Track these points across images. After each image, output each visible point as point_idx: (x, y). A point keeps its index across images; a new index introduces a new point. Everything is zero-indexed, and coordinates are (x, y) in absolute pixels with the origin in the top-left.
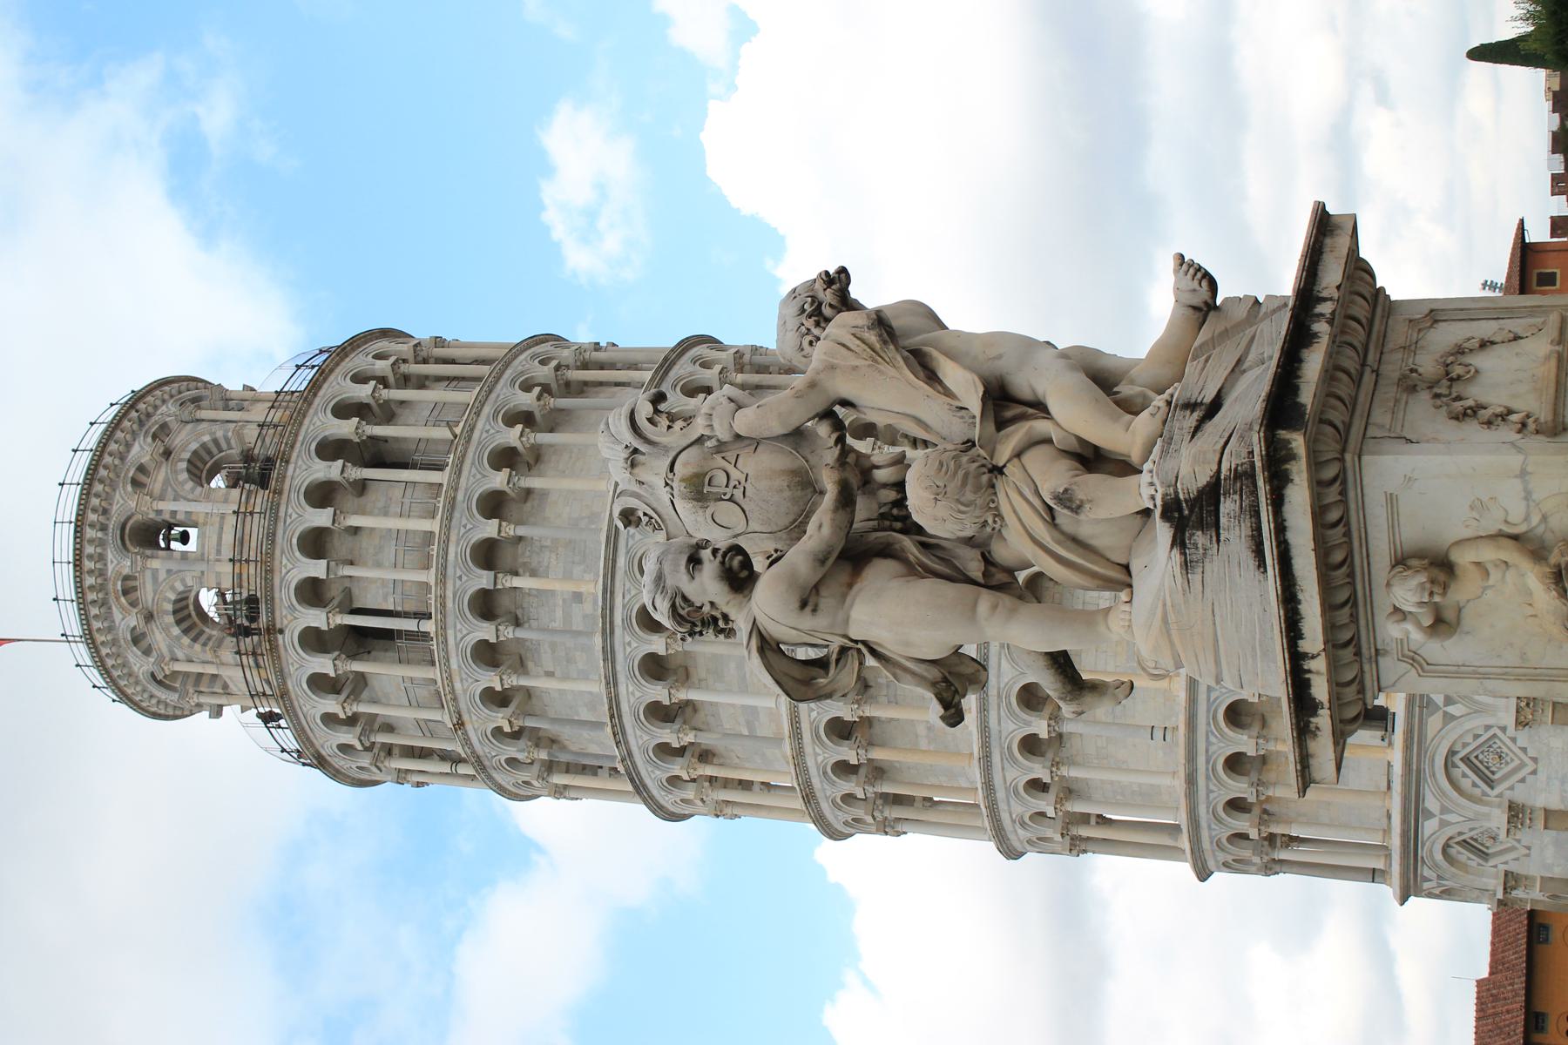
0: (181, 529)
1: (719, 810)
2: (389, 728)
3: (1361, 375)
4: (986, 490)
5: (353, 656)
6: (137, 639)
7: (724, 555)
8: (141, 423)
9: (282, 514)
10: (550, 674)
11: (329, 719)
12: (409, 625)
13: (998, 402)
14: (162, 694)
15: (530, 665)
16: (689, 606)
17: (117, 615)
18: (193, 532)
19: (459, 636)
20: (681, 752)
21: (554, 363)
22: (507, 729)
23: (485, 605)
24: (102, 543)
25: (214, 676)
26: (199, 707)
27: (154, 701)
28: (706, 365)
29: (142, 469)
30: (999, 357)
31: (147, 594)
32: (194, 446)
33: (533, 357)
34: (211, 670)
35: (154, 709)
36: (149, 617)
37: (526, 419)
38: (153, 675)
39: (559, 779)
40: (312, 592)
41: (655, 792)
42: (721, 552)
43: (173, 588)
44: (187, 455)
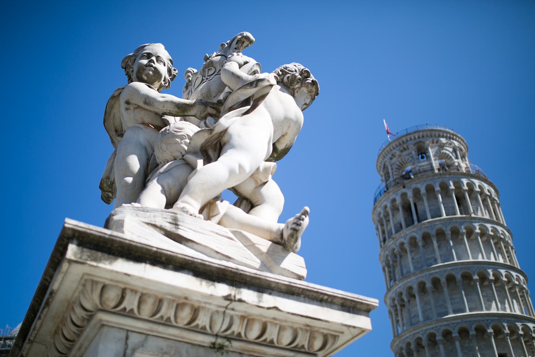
0: (425, 156)
1: (390, 313)
2: (388, 221)
3: (202, 331)
4: (171, 156)
5: (403, 207)
6: (393, 155)
7: (152, 66)
8: (450, 138)
9: (435, 177)
10: (413, 259)
11: (386, 207)
12: (415, 218)
13: (218, 146)
14: (382, 166)
15: (414, 253)
16: (132, 63)
17: (397, 148)
18: (425, 159)
19: (416, 231)
20: (403, 300)
21: (502, 237)
22: (395, 251)
23: (426, 237)
24: (415, 138)
25: (389, 177)
26: (382, 176)
27: (380, 165)
28: (517, 280)
29: (437, 142)
30: (239, 136)
31: (405, 153)
32: (448, 152)
33: (502, 231)
34: (391, 174)
35: (378, 165)
36: (400, 156)
37: (483, 233)
38: (386, 162)
39: (386, 269)
40: (417, 192)
41: (389, 295)
42: (153, 64)
43: (408, 159)
44: (444, 151)
